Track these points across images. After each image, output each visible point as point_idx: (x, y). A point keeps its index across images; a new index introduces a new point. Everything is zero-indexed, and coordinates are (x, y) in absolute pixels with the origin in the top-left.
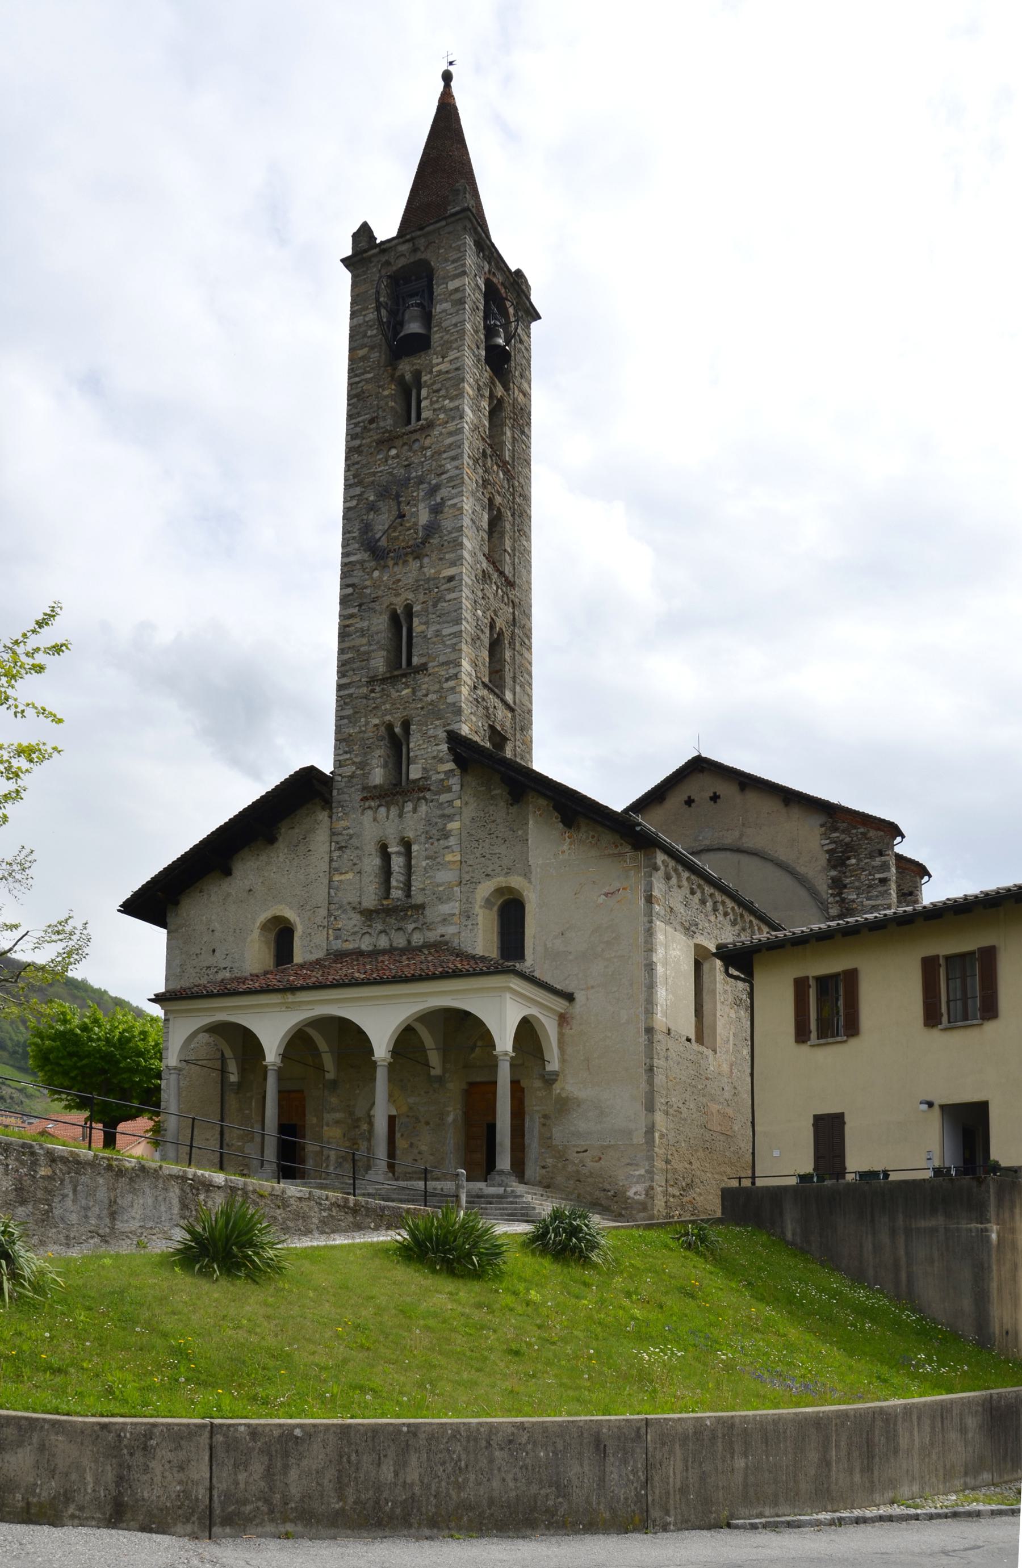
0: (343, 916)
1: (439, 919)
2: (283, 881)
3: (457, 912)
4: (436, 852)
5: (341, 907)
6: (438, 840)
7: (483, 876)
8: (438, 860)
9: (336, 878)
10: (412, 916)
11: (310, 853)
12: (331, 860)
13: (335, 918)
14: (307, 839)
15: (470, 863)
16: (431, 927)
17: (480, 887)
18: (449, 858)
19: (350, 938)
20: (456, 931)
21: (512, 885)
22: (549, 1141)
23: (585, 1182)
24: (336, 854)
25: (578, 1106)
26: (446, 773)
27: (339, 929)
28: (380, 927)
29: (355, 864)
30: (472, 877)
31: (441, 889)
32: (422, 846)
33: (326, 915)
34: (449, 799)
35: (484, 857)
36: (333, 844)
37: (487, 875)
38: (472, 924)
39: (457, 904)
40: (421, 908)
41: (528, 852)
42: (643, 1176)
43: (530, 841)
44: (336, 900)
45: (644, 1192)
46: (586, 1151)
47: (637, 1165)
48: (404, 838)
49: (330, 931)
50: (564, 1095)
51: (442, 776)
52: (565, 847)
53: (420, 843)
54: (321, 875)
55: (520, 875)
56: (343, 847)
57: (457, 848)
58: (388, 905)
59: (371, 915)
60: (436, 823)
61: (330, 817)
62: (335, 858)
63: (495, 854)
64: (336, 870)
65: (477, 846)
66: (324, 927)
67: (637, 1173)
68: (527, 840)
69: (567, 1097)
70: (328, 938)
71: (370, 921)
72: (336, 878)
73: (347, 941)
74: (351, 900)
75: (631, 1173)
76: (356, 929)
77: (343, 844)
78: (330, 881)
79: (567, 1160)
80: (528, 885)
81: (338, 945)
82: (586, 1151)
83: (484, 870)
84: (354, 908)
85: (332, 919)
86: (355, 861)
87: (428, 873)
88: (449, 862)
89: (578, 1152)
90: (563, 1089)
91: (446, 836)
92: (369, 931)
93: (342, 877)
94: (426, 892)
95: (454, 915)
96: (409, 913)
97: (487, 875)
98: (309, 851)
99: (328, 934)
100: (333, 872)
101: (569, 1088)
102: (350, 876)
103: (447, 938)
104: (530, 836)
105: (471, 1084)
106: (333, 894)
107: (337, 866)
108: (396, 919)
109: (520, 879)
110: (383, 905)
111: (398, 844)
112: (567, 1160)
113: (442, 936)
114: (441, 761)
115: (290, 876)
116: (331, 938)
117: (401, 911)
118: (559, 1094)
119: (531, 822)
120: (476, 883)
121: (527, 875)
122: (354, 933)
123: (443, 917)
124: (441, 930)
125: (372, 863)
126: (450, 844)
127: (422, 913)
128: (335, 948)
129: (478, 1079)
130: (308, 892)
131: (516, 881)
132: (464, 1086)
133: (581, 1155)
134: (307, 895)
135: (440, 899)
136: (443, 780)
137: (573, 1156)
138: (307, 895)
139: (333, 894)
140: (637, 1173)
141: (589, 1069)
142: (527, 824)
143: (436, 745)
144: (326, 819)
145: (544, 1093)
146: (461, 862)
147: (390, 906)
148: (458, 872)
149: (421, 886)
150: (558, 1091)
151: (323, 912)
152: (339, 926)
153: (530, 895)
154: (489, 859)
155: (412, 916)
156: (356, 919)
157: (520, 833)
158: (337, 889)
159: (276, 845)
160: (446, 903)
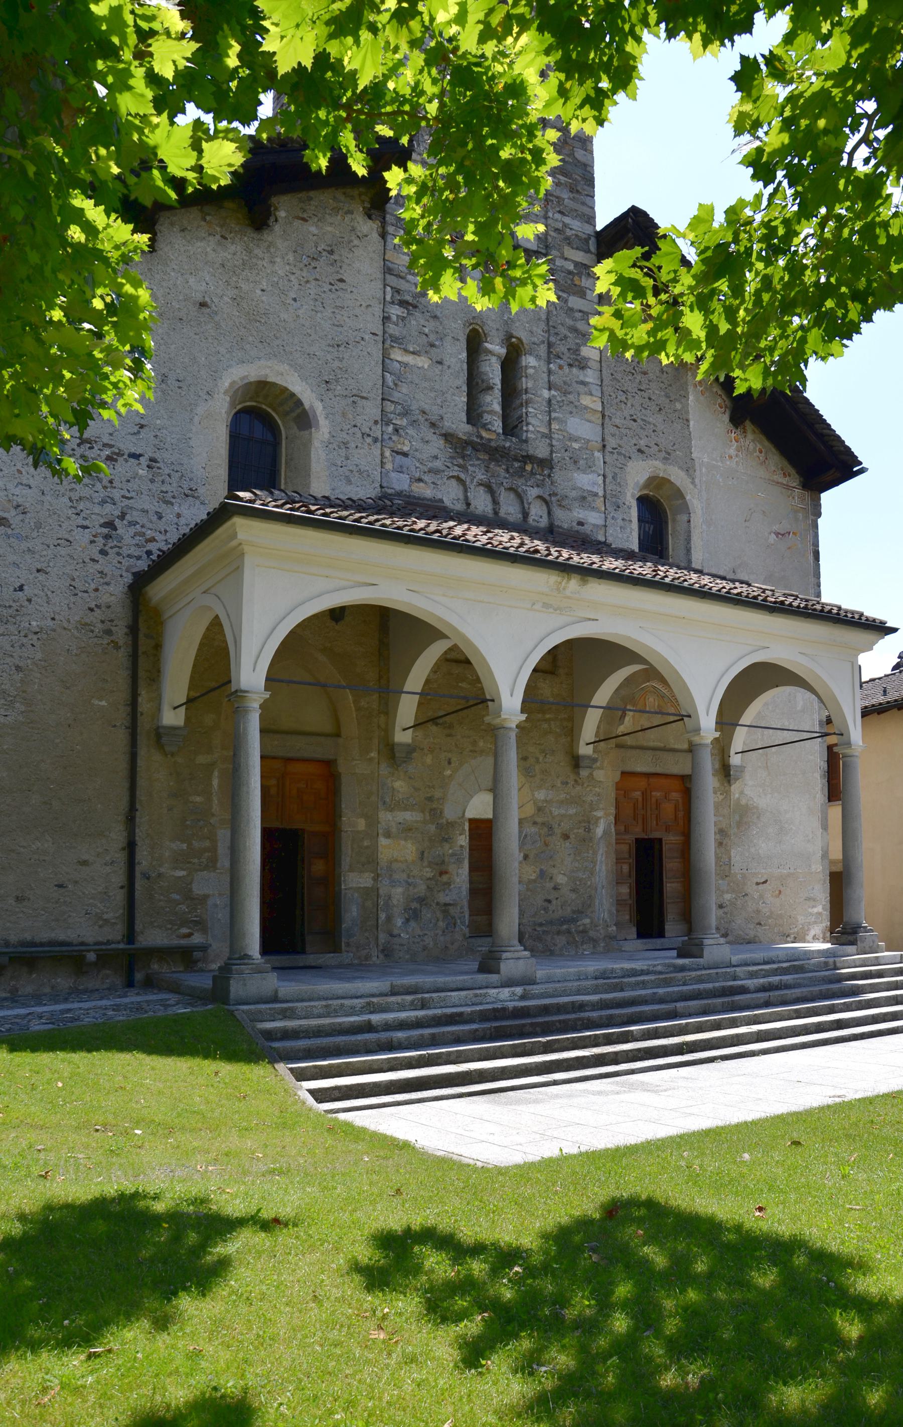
0: (411, 431)
1: (574, 494)
2: (284, 316)
3: (601, 493)
4: (565, 383)
5: (406, 413)
6: (570, 365)
7: (634, 449)
8: (571, 397)
9: (397, 355)
10: (532, 473)
11: (341, 285)
12: (386, 319)
13: (396, 430)
14: (335, 257)
15: (617, 421)
16: (564, 503)
17: (630, 464)
18: (586, 401)
19: (426, 478)
20: (601, 522)
21: (672, 479)
22: (727, 868)
23: (765, 925)
24: (396, 311)
25: (758, 818)
26: (576, 264)
27: (405, 455)
28: (481, 476)
29: (432, 345)
30: (620, 446)
31: (576, 446)
32: (542, 363)
33: (379, 418)
34: (585, 310)
35: (635, 421)
36: (388, 289)
37: (640, 451)
38: (623, 519)
39: (600, 480)
40: (546, 464)
41: (690, 440)
42: (820, 914)
43: (692, 423)
44: (396, 396)
45: (821, 936)
46: (765, 882)
47: (814, 900)
48: (511, 336)
49: (388, 453)
50: (743, 802)
51: (571, 267)
52: (732, 451)
53: (538, 357)
54: (367, 337)
55: (681, 468)
56: (407, 303)
57: (597, 391)
58: (490, 440)
59: (464, 448)
60: (566, 337)
61: (383, 235)
62: (394, 318)
63: (649, 423)
64: (395, 339)
65: (623, 399)
66: (376, 440)
67: (815, 910)
68: (688, 420)
69: (747, 805)
70: (383, 464)
71: (463, 458)
72: (397, 355)
73: (420, 480)
74: (427, 407)
75: (810, 910)
76: (438, 464)
77: (408, 298)
78: (385, 356)
79: (746, 895)
80: (691, 486)
81: (400, 483)
82: (765, 882)
83: (634, 441)
84: (433, 425)
85: (390, 429)
86: (432, 337)
87: (555, 411)
88: (586, 408)
89: (758, 884)
90: (742, 793)
91: (582, 364)
92: (463, 476)
93: (409, 359)
94: (554, 443)
95: (596, 495)
96: (528, 468)
97: (640, 451)
98: (341, 281)
99: (382, 455)
100: (388, 342)
101: (748, 791)
102: (422, 362)
103: (587, 529)
104: (691, 417)
105: (623, 773)
106: (391, 384)
107: (397, 334)
108: (507, 471)
109: (682, 474)
110: (482, 438)
111: (503, 343)
112: (746, 895)
113: (581, 524)
114: (568, 241)
115: (300, 312)
116: (389, 466)
117: (516, 460)
118: (738, 799)
119: (691, 398)
120: (625, 456)
121: (689, 469)
122: (432, 471)
123: (580, 493)
124: (579, 513)
125: (456, 355)
126: (587, 380)
127: (549, 476)
128: (398, 488)
129: (639, 769)
130: (341, 360)
131: (677, 476)
132: (617, 777)
133: (761, 887)
134: (337, 364)
135: (575, 462)
136: (570, 273)
137: (751, 889)
138: (337, 364)
139: (391, 384)
140: (815, 910)
141: (767, 767)
142: (686, 397)
143: (560, 212)
144: (375, 236)
145: (721, 797)
146: (603, 416)
147: (493, 444)
148: (599, 428)
149: (546, 431)
150: (737, 796)
151: (372, 410)
152: (406, 449)
153: (695, 502)
154: (642, 428)
155: (532, 473)
156: (437, 445)
157: (678, 406)
158: (399, 378)
159: (267, 236)
160: (584, 472)
